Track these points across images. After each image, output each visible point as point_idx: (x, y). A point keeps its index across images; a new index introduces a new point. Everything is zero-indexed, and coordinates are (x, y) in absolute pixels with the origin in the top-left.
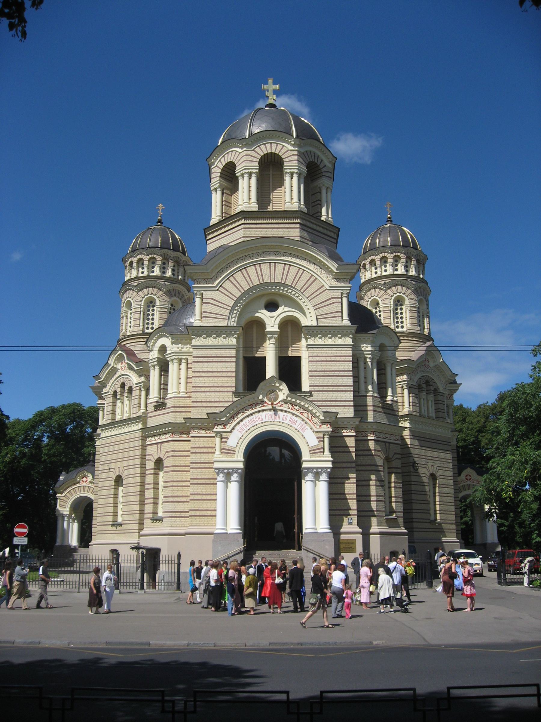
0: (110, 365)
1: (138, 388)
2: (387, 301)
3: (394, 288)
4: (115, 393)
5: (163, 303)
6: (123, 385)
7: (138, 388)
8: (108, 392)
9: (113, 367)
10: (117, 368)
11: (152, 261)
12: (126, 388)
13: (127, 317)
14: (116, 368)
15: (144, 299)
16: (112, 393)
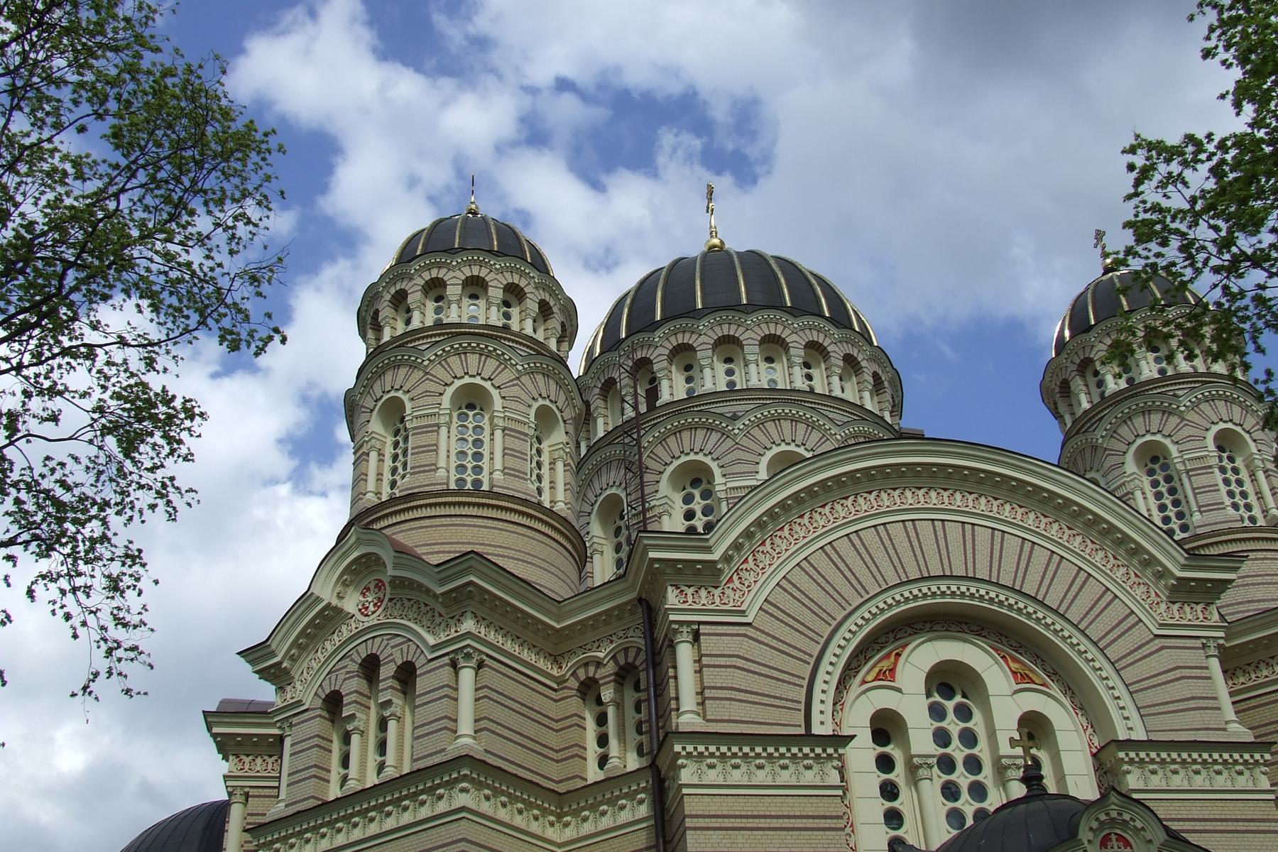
0: (319, 600)
1: (446, 660)
2: (1197, 444)
3: (1221, 404)
4: (333, 702)
5: (514, 405)
6: (370, 667)
7: (446, 660)
8: (299, 703)
9: (329, 604)
10: (342, 610)
11: (471, 290)
12: (387, 671)
13: (381, 454)
14: (338, 611)
15: (450, 391)
16: (319, 703)
